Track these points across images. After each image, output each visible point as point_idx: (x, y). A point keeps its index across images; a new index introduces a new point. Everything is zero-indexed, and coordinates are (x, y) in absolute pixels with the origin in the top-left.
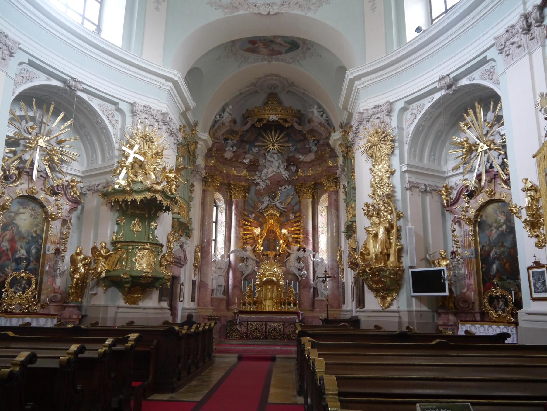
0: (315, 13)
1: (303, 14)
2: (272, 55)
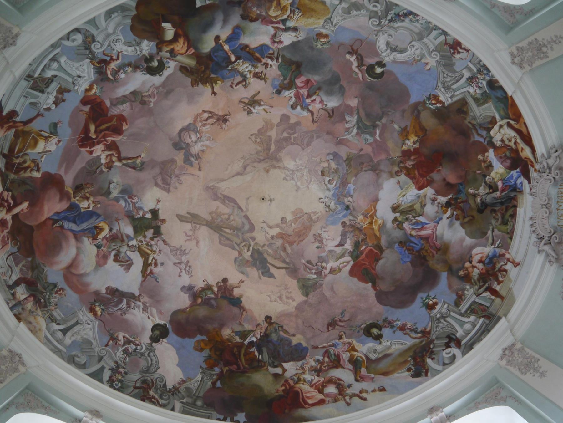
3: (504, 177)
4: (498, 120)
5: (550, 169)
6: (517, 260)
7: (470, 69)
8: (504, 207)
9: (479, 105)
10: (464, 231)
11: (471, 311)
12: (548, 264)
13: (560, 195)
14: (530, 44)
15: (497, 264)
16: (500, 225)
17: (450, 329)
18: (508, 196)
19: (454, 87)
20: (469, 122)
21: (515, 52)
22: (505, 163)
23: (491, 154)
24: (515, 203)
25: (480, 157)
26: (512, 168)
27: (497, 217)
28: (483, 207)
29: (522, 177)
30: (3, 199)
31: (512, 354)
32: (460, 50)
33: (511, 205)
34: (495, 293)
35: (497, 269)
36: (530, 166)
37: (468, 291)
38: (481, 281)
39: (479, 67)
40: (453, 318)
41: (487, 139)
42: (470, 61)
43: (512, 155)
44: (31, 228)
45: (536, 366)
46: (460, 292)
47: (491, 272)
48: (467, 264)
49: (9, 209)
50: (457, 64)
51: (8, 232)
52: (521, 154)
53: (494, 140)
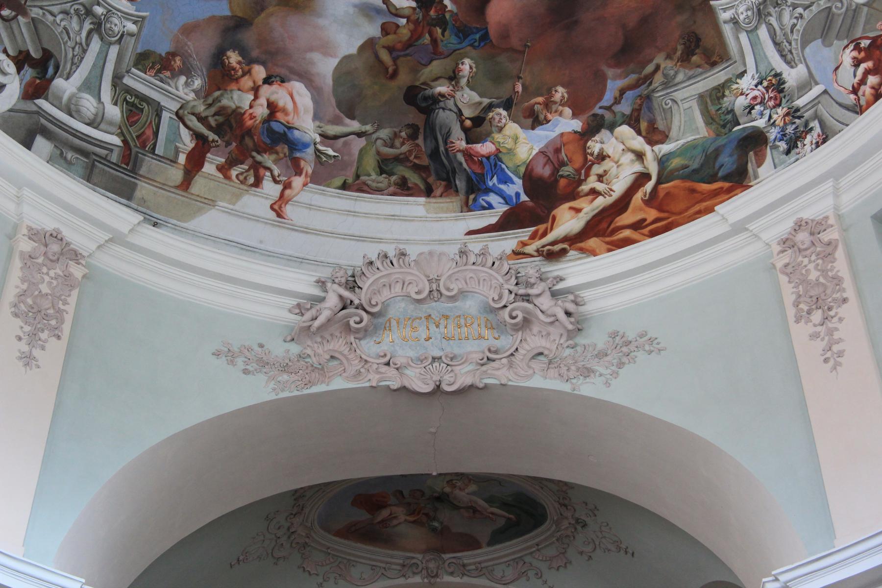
0: (607, 384)
1: (566, 387)
2: (442, 550)
3: (505, 158)
4: (656, 148)
5: (527, 298)
6: (288, 210)
7: (804, 87)
8: (425, 161)
9: (701, 97)
10: (353, 50)
11: (133, 104)
12: (294, 302)
13: (462, 321)
14: (838, 280)
15: (273, 157)
16: (378, 153)
17: (70, 55)
18: (454, 172)
19: (763, 33)
20: (658, 68)
21: (825, 237)
22: (542, 160)
23: (567, 123)
24: (438, 192)
25: (560, 93)
26: (530, 180)
27: (397, 143)
28: (420, 101)
29: (505, 208)
31: (52, 261)
32: (863, 66)
33: (431, 180)
34: (196, 161)
35: (259, 158)
36: (533, 229)
37: (187, 84)
38: (220, 119)
39: (807, 115)
40: (103, 57)
41: (608, 116)
42: (825, 92)
43: (563, 182)
45: (44, 336)
46: (178, 62)
47: (248, 141)
48: (260, 72)
50: (827, 52)
52: (567, 205)
53: (604, 134)
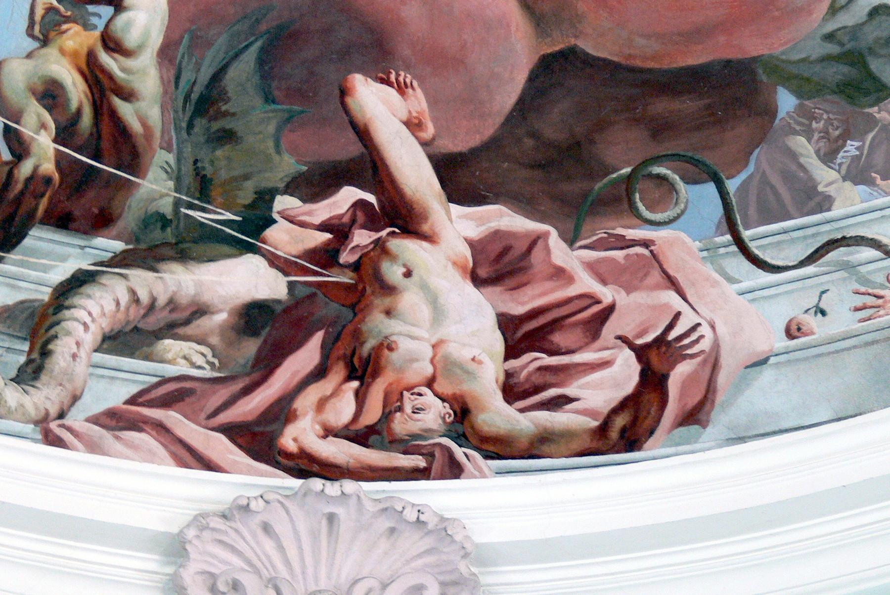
30: (325, 257)
44: (555, 70)
49: (398, 215)
51: (571, 241)
